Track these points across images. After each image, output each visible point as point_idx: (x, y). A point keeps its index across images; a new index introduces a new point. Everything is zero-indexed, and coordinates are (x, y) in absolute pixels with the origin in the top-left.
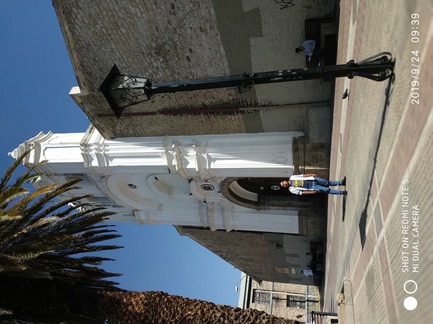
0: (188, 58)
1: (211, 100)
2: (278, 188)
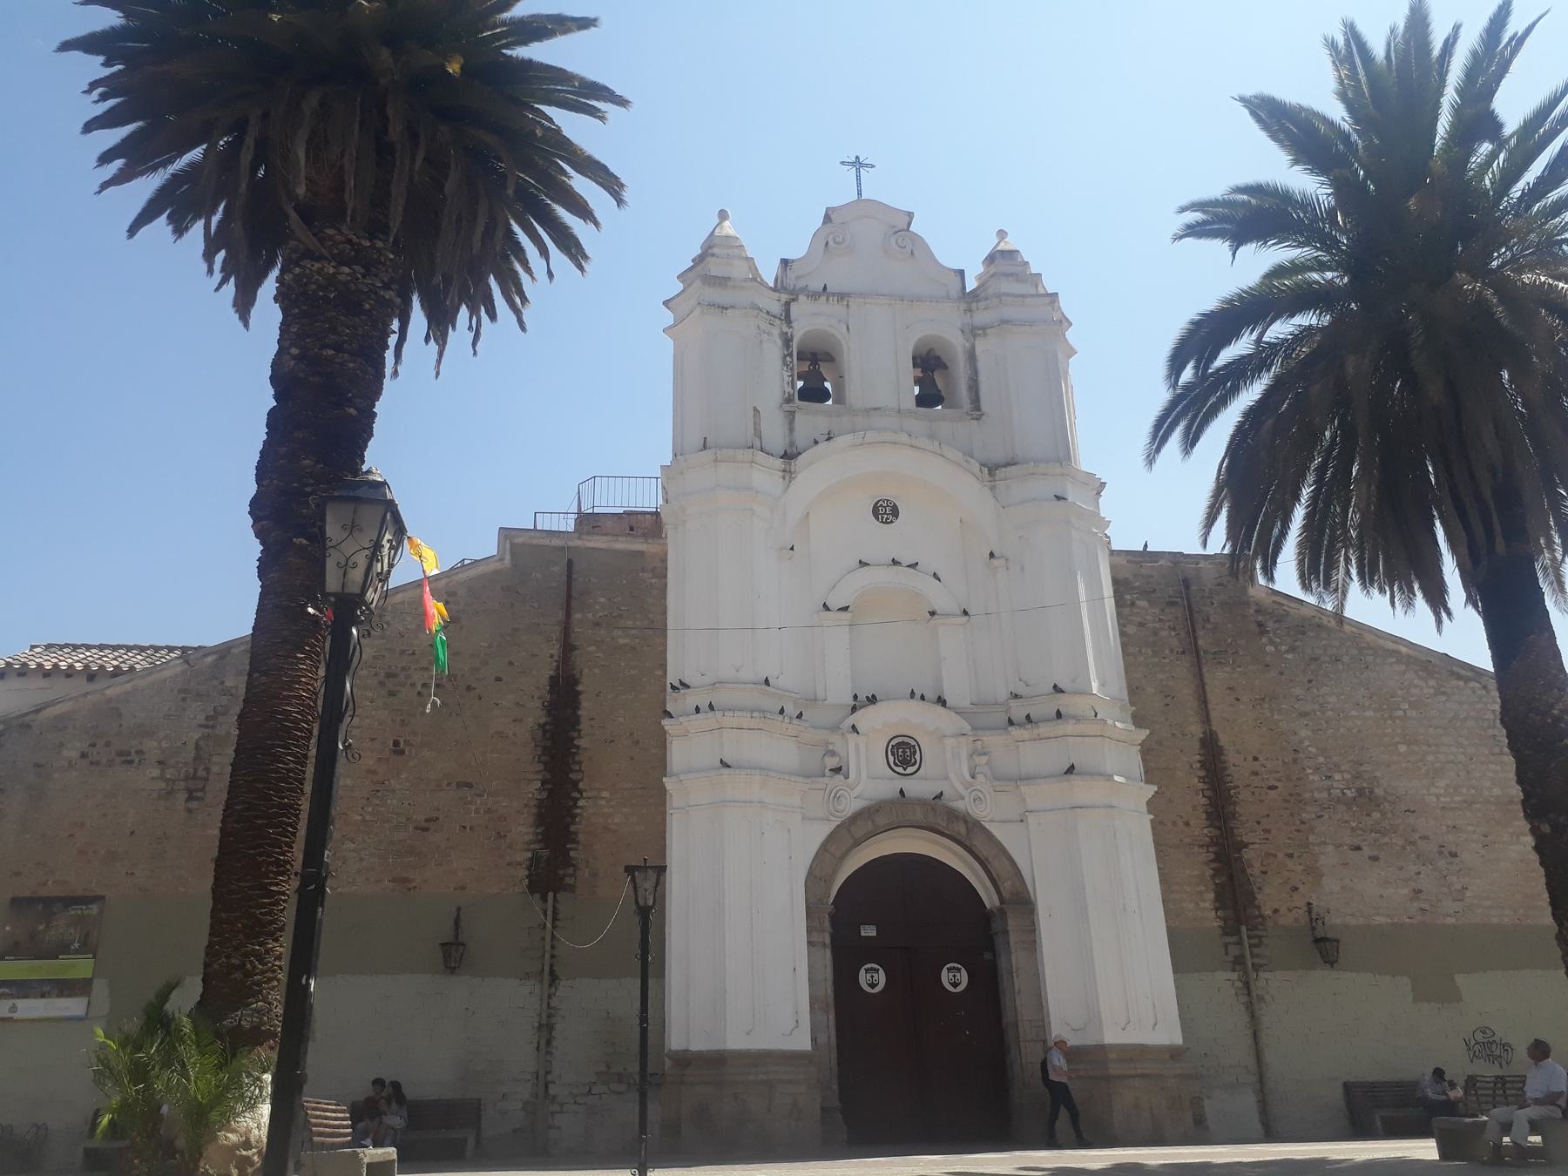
0: (1359, 848)
1: (1257, 865)
2: (873, 986)
